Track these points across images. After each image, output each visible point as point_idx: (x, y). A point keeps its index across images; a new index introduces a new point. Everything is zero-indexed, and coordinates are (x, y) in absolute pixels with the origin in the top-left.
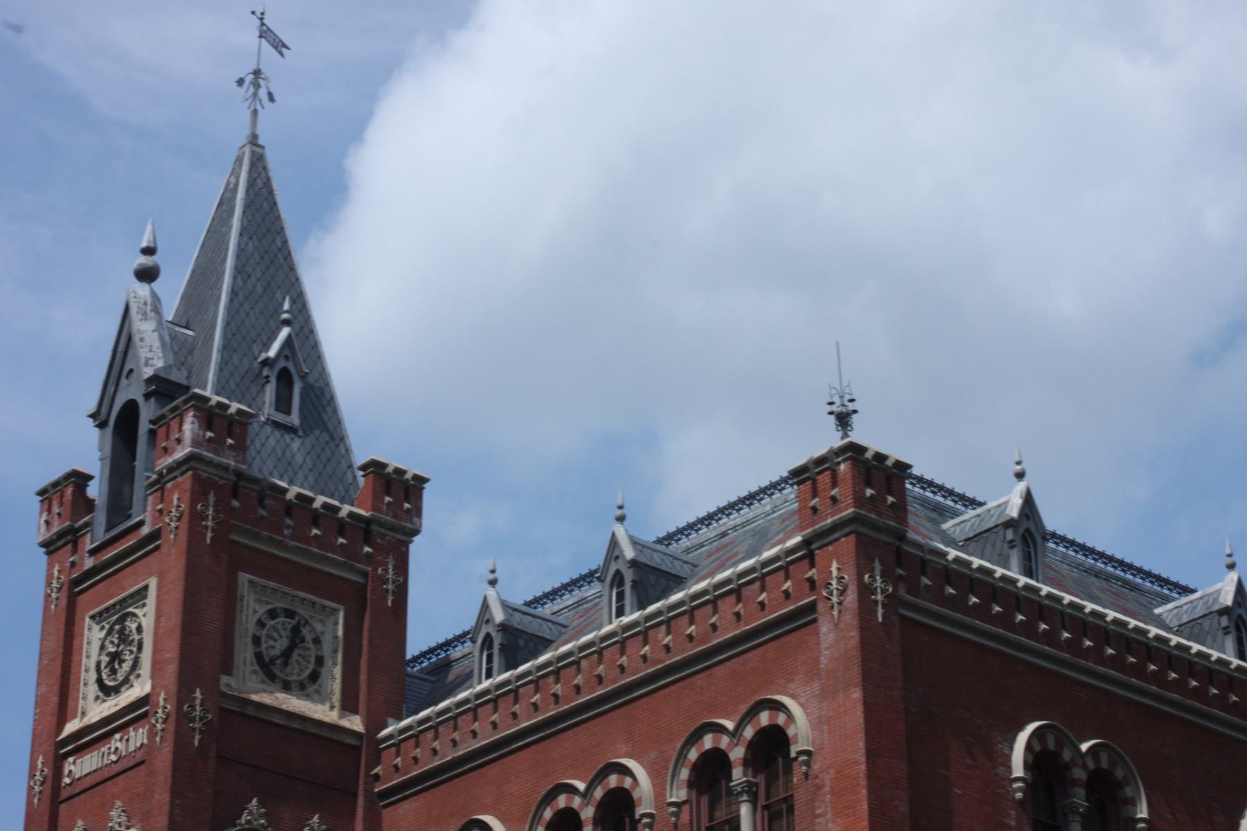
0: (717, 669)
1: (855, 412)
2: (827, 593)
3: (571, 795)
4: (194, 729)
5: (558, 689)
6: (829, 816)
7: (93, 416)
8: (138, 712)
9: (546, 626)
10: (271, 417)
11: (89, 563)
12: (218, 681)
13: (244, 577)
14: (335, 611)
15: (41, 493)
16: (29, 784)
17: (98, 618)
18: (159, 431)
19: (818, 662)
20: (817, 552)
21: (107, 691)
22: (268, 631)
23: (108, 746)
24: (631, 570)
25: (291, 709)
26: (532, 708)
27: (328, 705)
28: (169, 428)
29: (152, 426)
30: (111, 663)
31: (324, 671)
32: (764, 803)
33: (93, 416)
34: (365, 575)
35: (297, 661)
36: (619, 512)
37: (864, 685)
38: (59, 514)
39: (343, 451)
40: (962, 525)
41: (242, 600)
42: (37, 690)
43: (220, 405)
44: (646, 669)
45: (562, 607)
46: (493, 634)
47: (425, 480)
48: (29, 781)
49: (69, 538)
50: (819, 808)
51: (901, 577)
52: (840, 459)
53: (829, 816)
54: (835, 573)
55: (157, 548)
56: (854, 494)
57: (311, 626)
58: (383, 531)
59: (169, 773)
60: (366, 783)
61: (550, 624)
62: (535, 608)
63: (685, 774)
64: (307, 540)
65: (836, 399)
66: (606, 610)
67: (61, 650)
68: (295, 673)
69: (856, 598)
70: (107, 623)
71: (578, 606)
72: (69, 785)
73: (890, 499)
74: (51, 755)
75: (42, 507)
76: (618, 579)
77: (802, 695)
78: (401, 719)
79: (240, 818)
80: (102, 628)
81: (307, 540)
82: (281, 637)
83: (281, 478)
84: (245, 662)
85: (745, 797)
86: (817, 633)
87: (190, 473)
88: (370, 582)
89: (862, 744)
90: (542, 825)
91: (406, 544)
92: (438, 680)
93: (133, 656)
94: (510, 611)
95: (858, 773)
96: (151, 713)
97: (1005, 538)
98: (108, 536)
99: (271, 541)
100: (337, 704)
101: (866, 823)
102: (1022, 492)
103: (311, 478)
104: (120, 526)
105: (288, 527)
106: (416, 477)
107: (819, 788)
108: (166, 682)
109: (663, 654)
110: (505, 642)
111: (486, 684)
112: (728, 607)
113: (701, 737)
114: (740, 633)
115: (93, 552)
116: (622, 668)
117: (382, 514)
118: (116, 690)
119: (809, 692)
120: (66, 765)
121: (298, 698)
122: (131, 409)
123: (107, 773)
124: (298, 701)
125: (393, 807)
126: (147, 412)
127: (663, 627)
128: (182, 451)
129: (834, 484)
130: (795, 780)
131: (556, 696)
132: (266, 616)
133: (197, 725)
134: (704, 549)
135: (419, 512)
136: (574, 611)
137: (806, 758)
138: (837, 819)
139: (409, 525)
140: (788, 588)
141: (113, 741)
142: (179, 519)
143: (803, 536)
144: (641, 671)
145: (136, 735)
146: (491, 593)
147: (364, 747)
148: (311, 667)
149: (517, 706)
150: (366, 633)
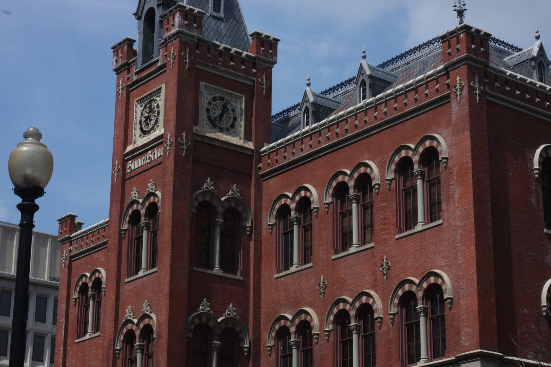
0: (407, 122)
1: (465, 10)
2: (455, 90)
3: (344, 176)
4: (183, 149)
5: (338, 130)
6: (456, 185)
7: (135, 15)
8: (158, 142)
9: (331, 103)
10: (212, 14)
11: (135, 78)
12: (192, 128)
13: (202, 83)
14: (241, 97)
15: (113, 48)
16: (112, 172)
17: (140, 101)
18: (164, 21)
19: (451, 119)
20: (450, 72)
21: (144, 133)
22: (213, 106)
23: (146, 156)
24: (369, 79)
25: (223, 140)
26: (327, 139)
27: (239, 138)
28: (168, 19)
29: (161, 19)
30: (146, 121)
31: (237, 123)
32: (427, 180)
33: (135, 15)
34: (253, 81)
35: (225, 119)
36: (363, 54)
37: (471, 129)
38: (122, 57)
39: (243, 28)
40: (512, 59)
41: (201, 93)
42: (114, 132)
43: (190, 9)
44: (376, 122)
45: (337, 94)
46: (309, 107)
47: (279, 40)
48: (112, 171)
49: (126, 67)
50: (451, 181)
51: (486, 83)
52: (460, 32)
53: (456, 185)
54: (458, 81)
55: (165, 71)
56: (467, 47)
57: (231, 104)
58: (260, 62)
59: (173, 168)
60: (255, 171)
61: (333, 102)
62: (326, 95)
63: (393, 167)
64: (228, 67)
65: (457, 4)
66: (358, 96)
67: (124, 115)
68: (225, 124)
69: (468, 92)
70: (144, 104)
71: (345, 94)
72: (130, 173)
73: (482, 49)
74: (121, 160)
75: (114, 54)
76: (363, 83)
77: (444, 133)
78: (270, 144)
79: (203, 186)
80: (142, 106)
81: (228, 67)
82: (218, 109)
83: (217, 40)
84: (203, 120)
85: (419, 177)
86: (450, 106)
87: (178, 39)
88: (255, 85)
89: (470, 155)
90: (332, 189)
91: (271, 68)
92: (284, 126)
93: (155, 118)
94: (316, 97)
95: (468, 167)
96: (164, 142)
97: (531, 65)
98: (143, 66)
99: (213, 68)
100: (242, 137)
101: (471, 188)
102: (538, 45)
103: (229, 40)
104: (148, 62)
105: (220, 62)
106: (274, 39)
107: (451, 173)
108: (170, 129)
109: (383, 116)
110: (315, 110)
111: (307, 128)
112: (412, 96)
113: (400, 151)
114: (417, 107)
115: (137, 73)
116: (366, 122)
117: (260, 55)
118: (149, 132)
119: (447, 132)
120: (128, 164)
121: (226, 135)
122: (151, 11)
123: (146, 168)
124: (226, 136)
125: (267, 181)
126: (159, 13)
127: (384, 104)
128: (175, 30)
129: (458, 43)
130: (441, 170)
131: (337, 134)
132: (212, 100)
133: (184, 147)
134: (399, 69)
135: (276, 54)
136: (343, 96)
137: (445, 160)
138: (459, 187)
139: (272, 60)
140: (438, 87)
141: (148, 154)
142: (174, 59)
143: (444, 65)
144: (374, 123)
145: (158, 151)
146: (308, 89)
147: (254, 155)
148: (231, 121)
149: (320, 138)
150: (254, 107)
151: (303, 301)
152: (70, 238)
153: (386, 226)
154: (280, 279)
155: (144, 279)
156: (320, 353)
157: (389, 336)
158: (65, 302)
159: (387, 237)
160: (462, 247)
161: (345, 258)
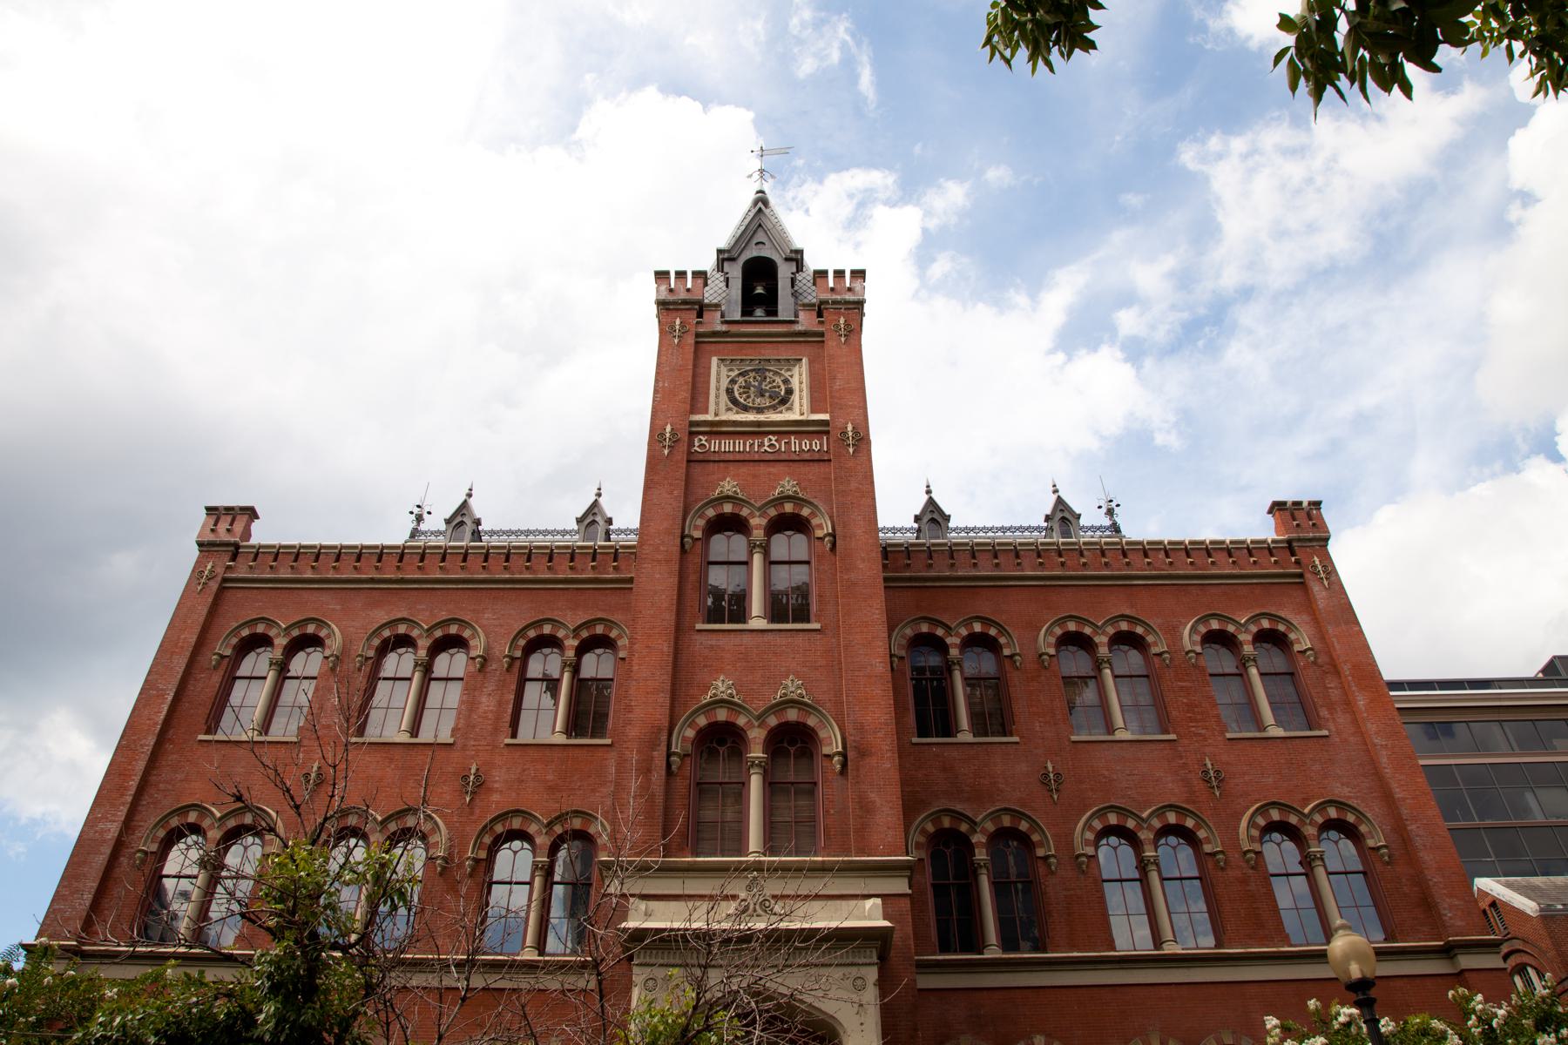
49: (697, 307)
70: (739, 370)
141: (766, 440)
151: (998, 795)
152: (237, 546)
153: (1199, 717)
154: (926, 747)
155: (770, 637)
156: (1065, 893)
157: (1248, 888)
158: (188, 654)
159: (1203, 731)
160: (1397, 775)
161: (1104, 745)
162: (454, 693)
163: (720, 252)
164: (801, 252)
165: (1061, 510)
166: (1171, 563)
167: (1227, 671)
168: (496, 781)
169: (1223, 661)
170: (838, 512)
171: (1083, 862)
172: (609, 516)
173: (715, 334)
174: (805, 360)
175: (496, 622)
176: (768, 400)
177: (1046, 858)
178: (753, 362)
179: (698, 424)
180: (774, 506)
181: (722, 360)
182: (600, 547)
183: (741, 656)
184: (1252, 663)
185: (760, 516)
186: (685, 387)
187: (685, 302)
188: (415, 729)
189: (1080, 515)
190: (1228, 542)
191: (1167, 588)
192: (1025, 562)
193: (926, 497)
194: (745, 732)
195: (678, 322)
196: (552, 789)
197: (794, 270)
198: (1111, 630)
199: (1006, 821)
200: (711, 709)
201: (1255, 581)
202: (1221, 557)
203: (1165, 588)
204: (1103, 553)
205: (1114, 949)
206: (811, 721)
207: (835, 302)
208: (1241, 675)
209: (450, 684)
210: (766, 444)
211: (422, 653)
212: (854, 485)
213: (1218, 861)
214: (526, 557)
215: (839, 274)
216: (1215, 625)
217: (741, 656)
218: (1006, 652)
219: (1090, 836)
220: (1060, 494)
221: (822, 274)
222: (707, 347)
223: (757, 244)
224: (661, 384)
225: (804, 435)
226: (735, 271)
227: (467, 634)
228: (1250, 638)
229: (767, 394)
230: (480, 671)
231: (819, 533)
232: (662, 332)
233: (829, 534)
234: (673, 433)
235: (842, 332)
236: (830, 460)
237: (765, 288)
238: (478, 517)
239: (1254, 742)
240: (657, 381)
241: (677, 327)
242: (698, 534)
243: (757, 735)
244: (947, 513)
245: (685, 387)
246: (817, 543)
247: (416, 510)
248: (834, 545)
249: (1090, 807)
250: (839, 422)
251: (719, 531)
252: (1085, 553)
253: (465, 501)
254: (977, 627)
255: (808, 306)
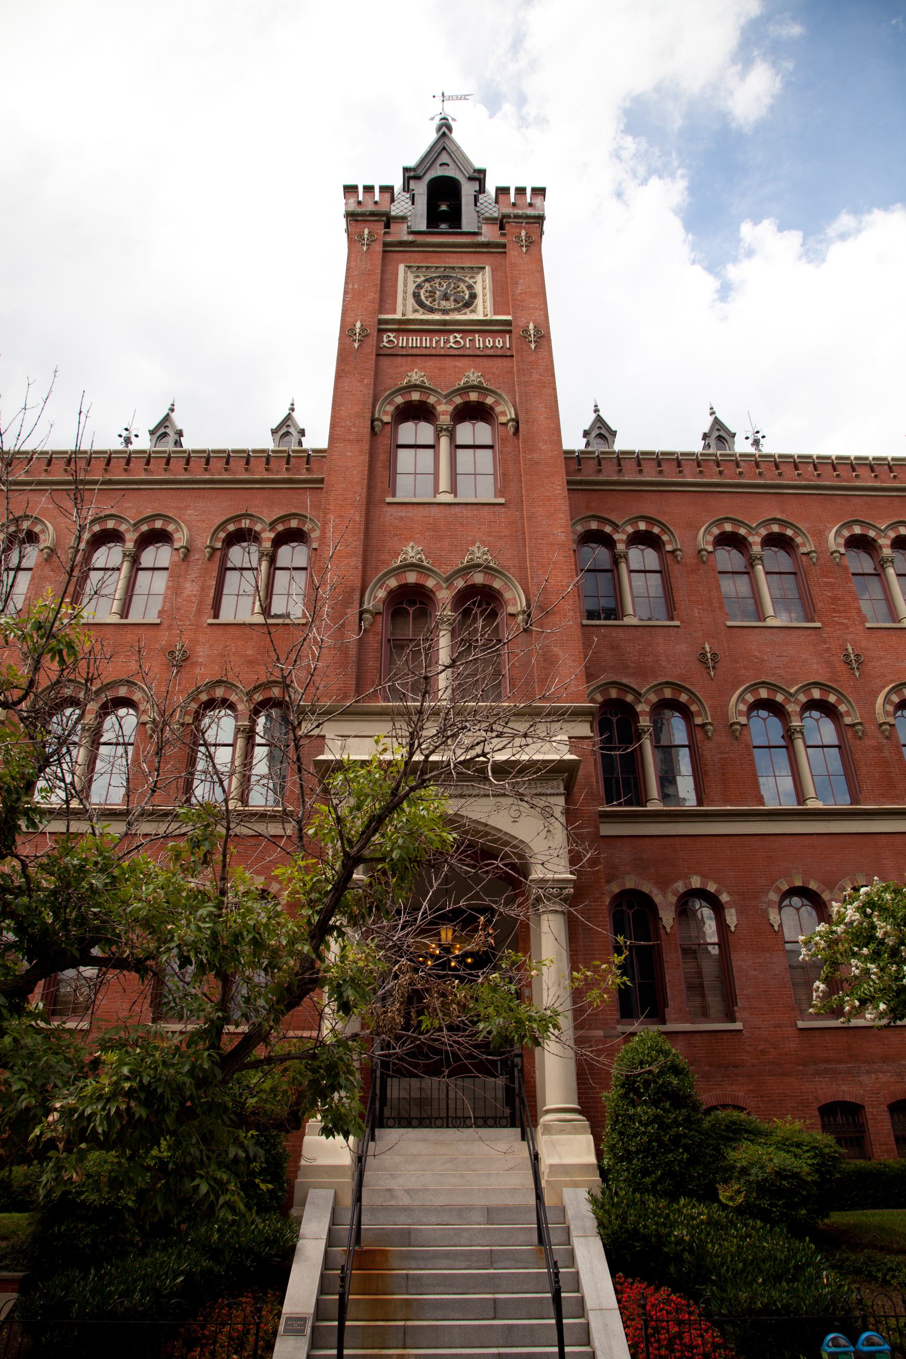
49: (384, 219)
70: (425, 276)
153: (842, 609)
154: (596, 629)
156: (720, 756)
157: (883, 755)
159: (845, 621)
161: (756, 630)
162: (159, 583)
163: (406, 170)
164: (483, 172)
165: (718, 430)
166: (819, 475)
167: (866, 571)
168: (199, 657)
169: (863, 563)
170: (521, 399)
171: (737, 730)
172: (301, 427)
173: (401, 244)
174: (487, 268)
175: (198, 518)
176: (453, 303)
177: (703, 726)
178: (438, 270)
179: (387, 322)
180: (460, 395)
181: (409, 267)
182: (294, 451)
183: (429, 526)
184: (890, 564)
185: (446, 403)
186: (374, 289)
187: (373, 214)
188: (125, 612)
189: (735, 434)
190: (871, 459)
191: (815, 497)
192: (686, 470)
193: (594, 416)
194: (434, 594)
195: (366, 231)
196: (251, 663)
197: (477, 188)
198: (763, 532)
199: (668, 693)
200: (401, 572)
201: (894, 494)
202: (864, 472)
203: (812, 497)
204: (757, 465)
205: (763, 804)
206: (497, 584)
207: (517, 216)
208: (878, 575)
209: (156, 573)
210: (452, 340)
211: (130, 545)
212: (535, 376)
213: (857, 732)
214: (225, 460)
215: (521, 191)
216: (857, 530)
217: (429, 526)
218: (669, 548)
219: (743, 707)
220: (717, 415)
221: (502, 191)
222: (395, 256)
223: (441, 165)
224: (350, 286)
225: (487, 334)
226: (421, 189)
227: (171, 528)
228: (888, 542)
229: (452, 298)
230: (183, 560)
231: (503, 419)
232: (350, 240)
233: (512, 420)
234: (363, 329)
235: (524, 243)
236: (512, 356)
237: (448, 206)
238: (179, 428)
239: (890, 632)
240: (346, 283)
241: (366, 236)
242: (387, 419)
243: (444, 596)
244: (614, 429)
245: (374, 289)
246: (501, 428)
247: (125, 433)
248: (517, 429)
249: (743, 683)
250: (522, 322)
251: (406, 420)
252: (742, 464)
253: (168, 414)
254: (642, 526)
255: (490, 220)
